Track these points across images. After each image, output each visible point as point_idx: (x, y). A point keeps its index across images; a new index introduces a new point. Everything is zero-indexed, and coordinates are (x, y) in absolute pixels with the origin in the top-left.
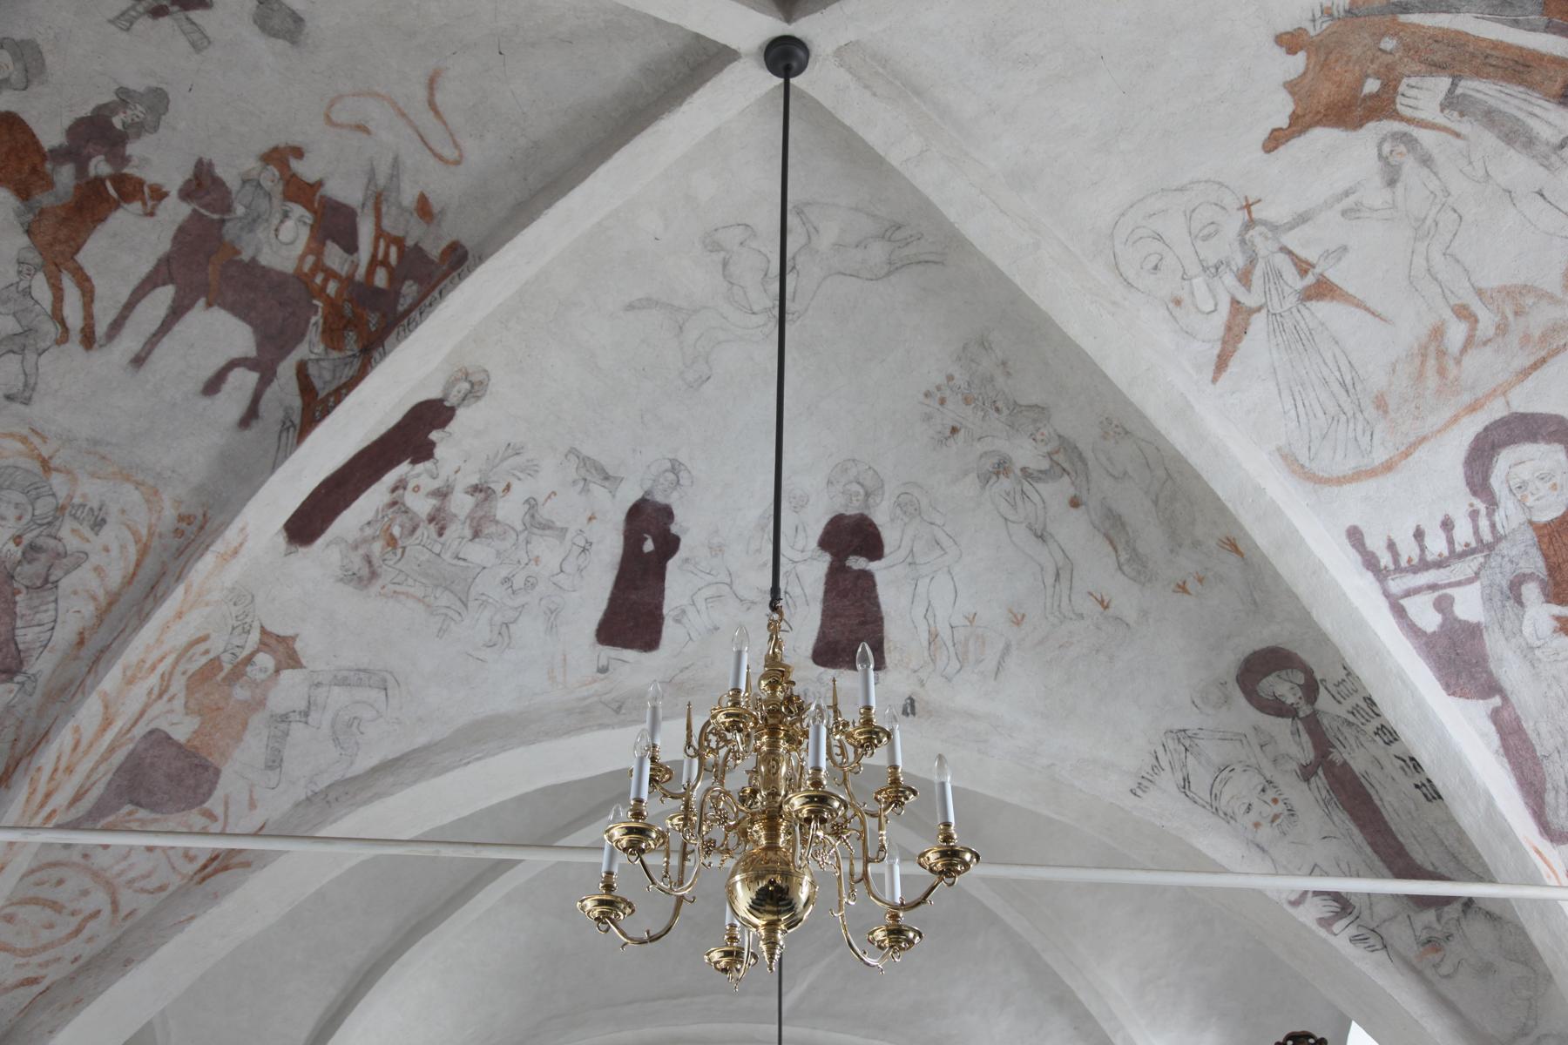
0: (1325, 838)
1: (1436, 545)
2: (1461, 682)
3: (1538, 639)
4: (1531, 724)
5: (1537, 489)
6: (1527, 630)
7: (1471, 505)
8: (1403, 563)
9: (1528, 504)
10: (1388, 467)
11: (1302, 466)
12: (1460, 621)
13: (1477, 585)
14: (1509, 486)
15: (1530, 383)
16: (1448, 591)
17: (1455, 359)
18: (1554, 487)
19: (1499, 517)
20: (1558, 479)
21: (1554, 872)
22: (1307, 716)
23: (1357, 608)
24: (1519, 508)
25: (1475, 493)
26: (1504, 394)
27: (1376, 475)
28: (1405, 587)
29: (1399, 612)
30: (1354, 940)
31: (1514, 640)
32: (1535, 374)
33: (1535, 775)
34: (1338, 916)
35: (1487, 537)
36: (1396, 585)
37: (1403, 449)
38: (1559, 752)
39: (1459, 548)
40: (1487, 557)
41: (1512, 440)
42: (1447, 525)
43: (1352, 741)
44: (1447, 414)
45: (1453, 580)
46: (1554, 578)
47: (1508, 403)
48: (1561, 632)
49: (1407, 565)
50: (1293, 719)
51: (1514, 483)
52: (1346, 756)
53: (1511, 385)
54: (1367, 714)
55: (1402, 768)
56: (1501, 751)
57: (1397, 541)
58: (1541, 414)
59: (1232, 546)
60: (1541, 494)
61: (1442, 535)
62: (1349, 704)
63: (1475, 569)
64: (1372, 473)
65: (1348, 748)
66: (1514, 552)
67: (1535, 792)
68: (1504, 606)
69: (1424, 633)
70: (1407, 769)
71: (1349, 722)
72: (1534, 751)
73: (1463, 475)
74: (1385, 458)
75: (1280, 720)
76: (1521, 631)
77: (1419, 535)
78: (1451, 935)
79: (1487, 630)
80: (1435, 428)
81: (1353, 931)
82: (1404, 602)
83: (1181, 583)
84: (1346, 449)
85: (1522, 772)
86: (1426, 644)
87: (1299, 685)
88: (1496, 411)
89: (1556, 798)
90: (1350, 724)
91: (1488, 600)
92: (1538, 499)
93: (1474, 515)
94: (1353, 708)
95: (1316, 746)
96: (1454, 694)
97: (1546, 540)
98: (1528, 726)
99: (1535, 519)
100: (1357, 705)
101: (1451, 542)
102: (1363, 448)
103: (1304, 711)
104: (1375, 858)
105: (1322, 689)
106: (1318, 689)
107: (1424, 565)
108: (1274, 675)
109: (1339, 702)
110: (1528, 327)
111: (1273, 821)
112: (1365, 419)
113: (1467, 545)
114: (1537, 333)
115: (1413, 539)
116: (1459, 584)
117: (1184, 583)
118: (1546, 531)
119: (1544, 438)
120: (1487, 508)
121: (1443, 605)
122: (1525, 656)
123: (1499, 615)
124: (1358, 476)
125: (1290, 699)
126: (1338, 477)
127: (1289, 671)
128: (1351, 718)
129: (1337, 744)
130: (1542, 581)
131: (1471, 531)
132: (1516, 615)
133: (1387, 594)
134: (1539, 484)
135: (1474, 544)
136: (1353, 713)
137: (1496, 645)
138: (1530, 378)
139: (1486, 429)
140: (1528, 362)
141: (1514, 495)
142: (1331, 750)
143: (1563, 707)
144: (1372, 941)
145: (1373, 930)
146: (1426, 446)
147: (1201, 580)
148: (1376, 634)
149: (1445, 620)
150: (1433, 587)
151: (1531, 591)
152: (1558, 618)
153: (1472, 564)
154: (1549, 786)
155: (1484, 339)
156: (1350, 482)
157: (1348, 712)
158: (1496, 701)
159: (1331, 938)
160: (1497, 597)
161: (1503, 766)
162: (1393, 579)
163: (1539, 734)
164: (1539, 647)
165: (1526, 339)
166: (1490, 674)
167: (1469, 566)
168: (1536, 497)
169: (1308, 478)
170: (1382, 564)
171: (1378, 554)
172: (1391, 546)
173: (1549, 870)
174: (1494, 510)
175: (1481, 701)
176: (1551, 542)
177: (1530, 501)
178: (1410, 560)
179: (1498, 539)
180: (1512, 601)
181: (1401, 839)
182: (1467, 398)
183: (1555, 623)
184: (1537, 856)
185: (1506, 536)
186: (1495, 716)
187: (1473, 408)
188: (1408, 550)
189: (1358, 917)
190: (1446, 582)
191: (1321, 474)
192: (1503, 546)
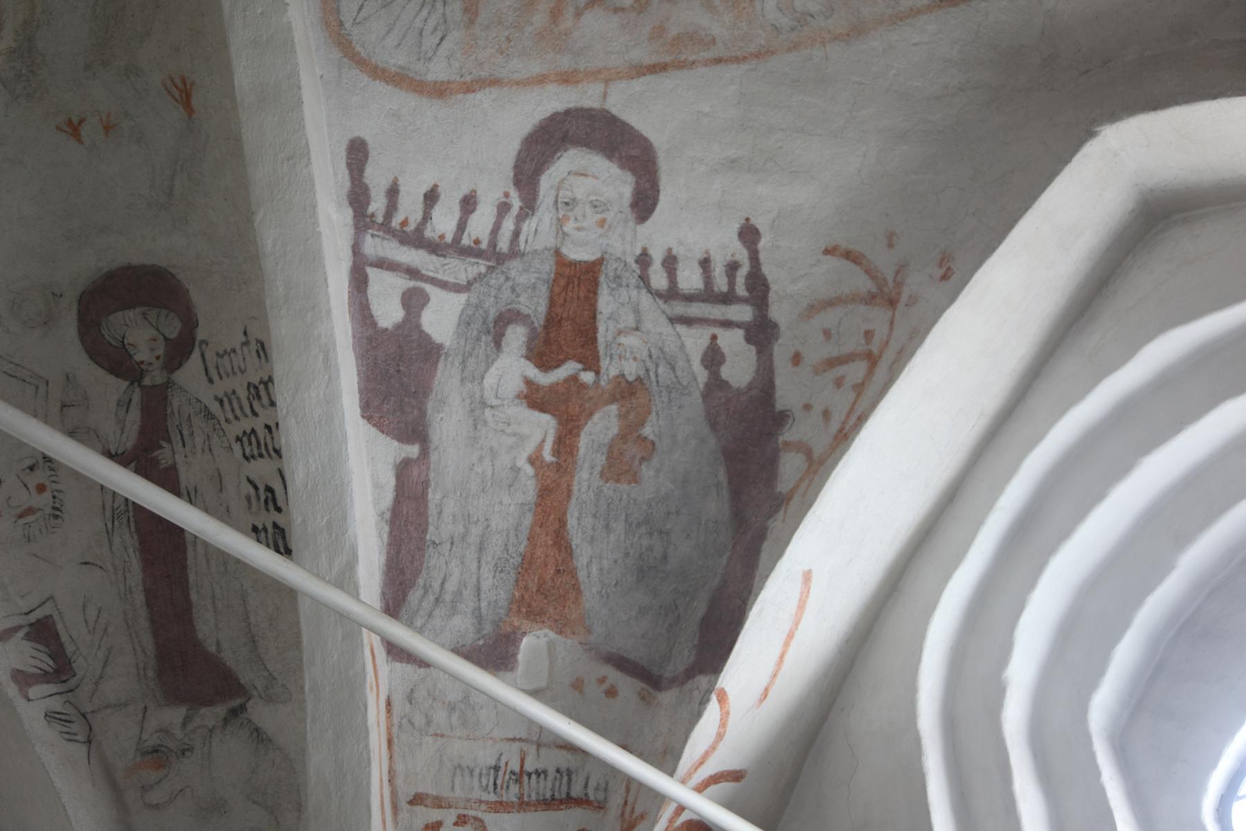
0: (86, 563)
1: (444, 223)
2: (385, 407)
3: (497, 397)
4: (438, 496)
5: (584, 216)
6: (490, 380)
7: (507, 195)
8: (395, 223)
9: (565, 229)
10: (440, 91)
11: (341, 24)
12: (421, 332)
13: (463, 298)
14: (557, 197)
15: (638, 85)
16: (428, 288)
17: (577, 8)
18: (602, 223)
19: (528, 227)
20: (609, 216)
21: (378, 686)
22: (154, 386)
23: (320, 234)
24: (554, 229)
25: (517, 183)
26: (607, 82)
27: (422, 93)
28: (381, 254)
29: (359, 282)
30: (50, 716)
31: (470, 385)
32: (648, 78)
33: (412, 562)
34: (45, 677)
35: (503, 245)
36: (374, 246)
37: (468, 79)
38: (452, 543)
39: (466, 241)
40: (491, 269)
41: (586, 142)
42: (469, 204)
43: (199, 440)
44: (536, 67)
45: (440, 277)
46: (548, 333)
47: (605, 95)
48: (524, 401)
49: (398, 227)
50: (132, 383)
51: (565, 195)
52: (179, 459)
53: (619, 76)
54: (241, 408)
55: (248, 498)
56: (388, 515)
57: (402, 189)
58: (632, 128)
59: (184, 94)
60: (585, 224)
61: (457, 214)
62: (221, 387)
63: (470, 276)
64: (419, 87)
65: (188, 448)
66: (522, 280)
67: (401, 584)
68: (478, 339)
69: (374, 324)
70: (254, 500)
71: (209, 413)
72: (425, 531)
73: (515, 153)
74: (443, 76)
75: (112, 379)
76: (483, 378)
77: (431, 197)
78: (191, 749)
79: (446, 359)
80: (515, 76)
81: (56, 704)
82: (372, 272)
83: (75, 121)
84: (404, 36)
85: (398, 552)
86: (370, 339)
87: (166, 338)
88: (587, 96)
89: (420, 602)
90: (209, 415)
91: (465, 322)
92: (578, 229)
93: (504, 208)
94: (226, 394)
95: (143, 431)
96: (369, 418)
97: (562, 282)
98: (434, 497)
99: (564, 251)
100: (234, 392)
101: (462, 227)
102: (424, 48)
103: (155, 377)
104: (143, 613)
105: (196, 355)
106: (190, 353)
107: (416, 239)
108: (138, 310)
109: (211, 381)
110: (668, 19)
111: (21, 516)
112: (444, 14)
113: (477, 242)
114: (673, 31)
115: (421, 198)
116: (444, 285)
117: (81, 121)
118: (567, 272)
119: (620, 159)
120: (521, 208)
121: (413, 302)
122: (472, 411)
123: (468, 348)
124: (400, 79)
125: (142, 355)
126: (376, 67)
127: (164, 312)
128: (215, 407)
129: (176, 438)
130: (533, 330)
131: (490, 227)
132: (487, 356)
133: (356, 249)
134: (589, 210)
135: (484, 246)
136: (221, 402)
137: (447, 380)
138: (642, 79)
139: (568, 112)
140: (648, 60)
141: (557, 209)
142: (164, 444)
143: (483, 490)
144: (74, 728)
145: (84, 715)
146: (494, 92)
147: (108, 128)
148: (326, 280)
149: (406, 320)
150: (412, 273)
151: (516, 336)
152: (529, 382)
153: (469, 269)
154: (420, 581)
155: (618, 5)
156: (387, 83)
157: (216, 398)
158: (413, 450)
159: (20, 703)
160: (476, 326)
161: (380, 535)
162: (373, 236)
163: (440, 513)
164: (492, 407)
165: (659, 32)
166: (423, 414)
167: (466, 270)
168: (578, 225)
169: (340, 44)
170: (372, 208)
171: (373, 193)
172: (393, 192)
173: (374, 684)
174: (527, 215)
175: (396, 443)
176: (565, 288)
177: (569, 227)
178: (405, 223)
179: (514, 253)
180: (490, 338)
181: (193, 596)
182: (565, 62)
183: (522, 387)
184: (370, 658)
185: (523, 254)
186: (403, 469)
187: (567, 78)
188: (410, 208)
189: (71, 691)
190: (431, 274)
191: (358, 48)
192: (515, 264)
